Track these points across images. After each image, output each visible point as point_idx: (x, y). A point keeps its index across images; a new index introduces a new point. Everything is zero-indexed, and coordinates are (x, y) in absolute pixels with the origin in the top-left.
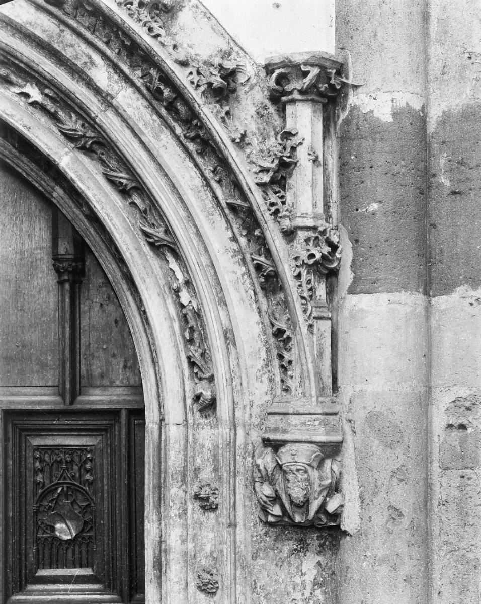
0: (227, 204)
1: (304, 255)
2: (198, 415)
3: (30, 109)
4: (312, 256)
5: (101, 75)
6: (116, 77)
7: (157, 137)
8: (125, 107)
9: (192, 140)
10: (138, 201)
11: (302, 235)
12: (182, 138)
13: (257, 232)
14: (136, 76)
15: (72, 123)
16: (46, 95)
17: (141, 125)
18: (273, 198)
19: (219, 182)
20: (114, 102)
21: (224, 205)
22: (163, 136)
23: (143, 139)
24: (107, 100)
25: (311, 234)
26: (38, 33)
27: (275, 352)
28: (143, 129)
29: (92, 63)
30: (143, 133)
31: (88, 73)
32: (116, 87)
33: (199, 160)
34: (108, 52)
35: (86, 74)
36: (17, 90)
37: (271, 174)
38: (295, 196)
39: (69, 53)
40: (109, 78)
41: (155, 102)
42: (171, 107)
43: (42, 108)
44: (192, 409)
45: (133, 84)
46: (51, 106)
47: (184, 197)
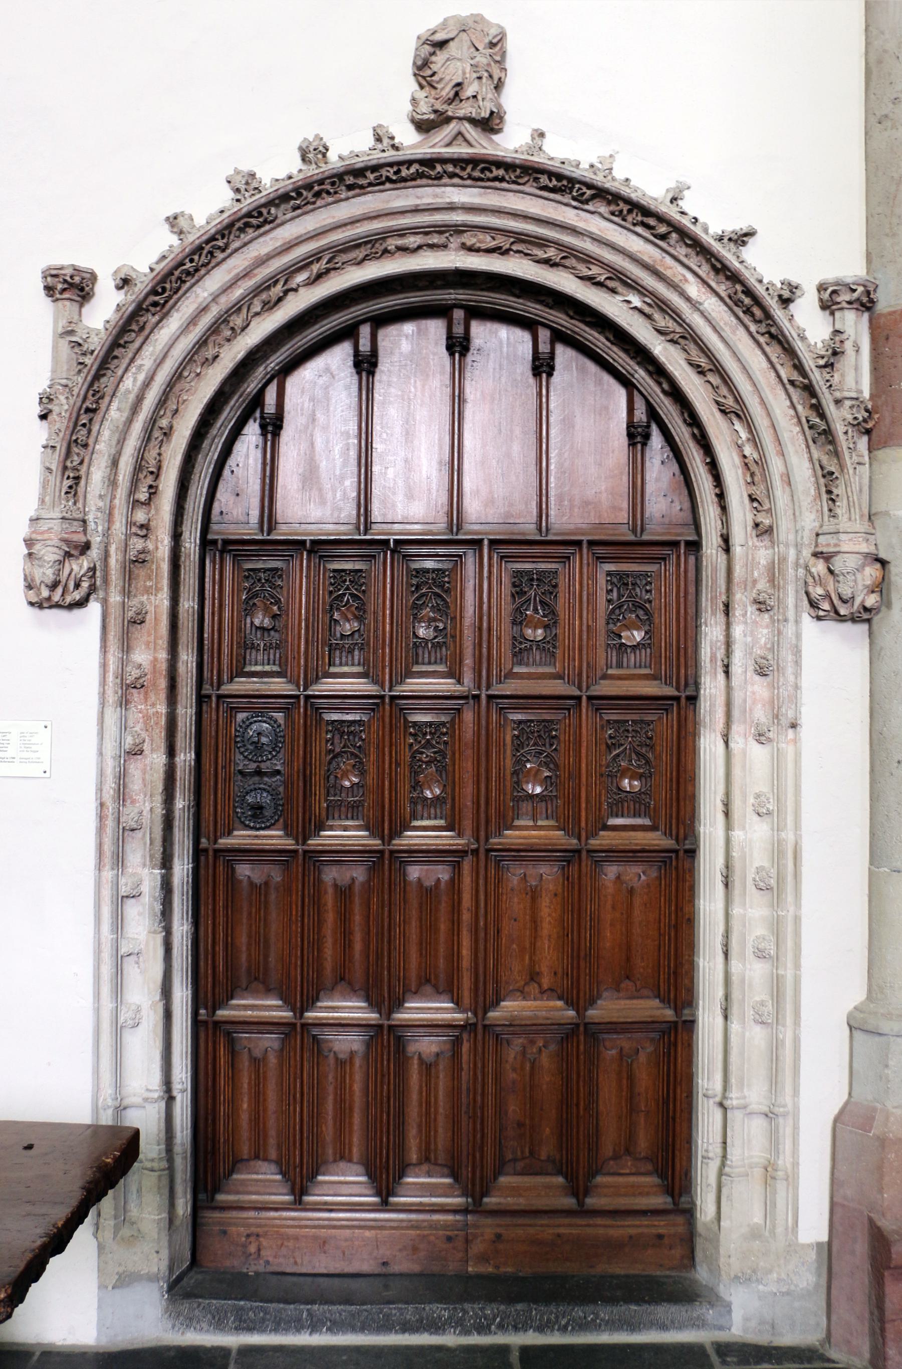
0: (789, 381)
1: (850, 418)
2: (755, 539)
3: (631, 311)
4: (855, 418)
5: (694, 289)
6: (704, 290)
7: (734, 332)
8: (710, 311)
9: (763, 334)
10: (711, 379)
11: (848, 403)
12: (755, 334)
13: (814, 401)
14: (722, 289)
15: (662, 321)
16: (644, 302)
17: (722, 324)
18: (828, 377)
19: (782, 365)
20: (701, 308)
21: (786, 381)
22: (738, 332)
23: (723, 334)
24: (695, 305)
25: (854, 402)
26: (646, 258)
27: (823, 489)
28: (723, 326)
29: (686, 280)
30: (723, 330)
31: (683, 287)
32: (704, 298)
33: (768, 349)
34: (700, 272)
35: (680, 287)
36: (622, 298)
37: (825, 360)
38: (843, 375)
39: (668, 273)
40: (698, 291)
41: (736, 309)
42: (748, 311)
43: (640, 311)
44: (751, 535)
45: (717, 294)
46: (647, 309)
47: (753, 377)
